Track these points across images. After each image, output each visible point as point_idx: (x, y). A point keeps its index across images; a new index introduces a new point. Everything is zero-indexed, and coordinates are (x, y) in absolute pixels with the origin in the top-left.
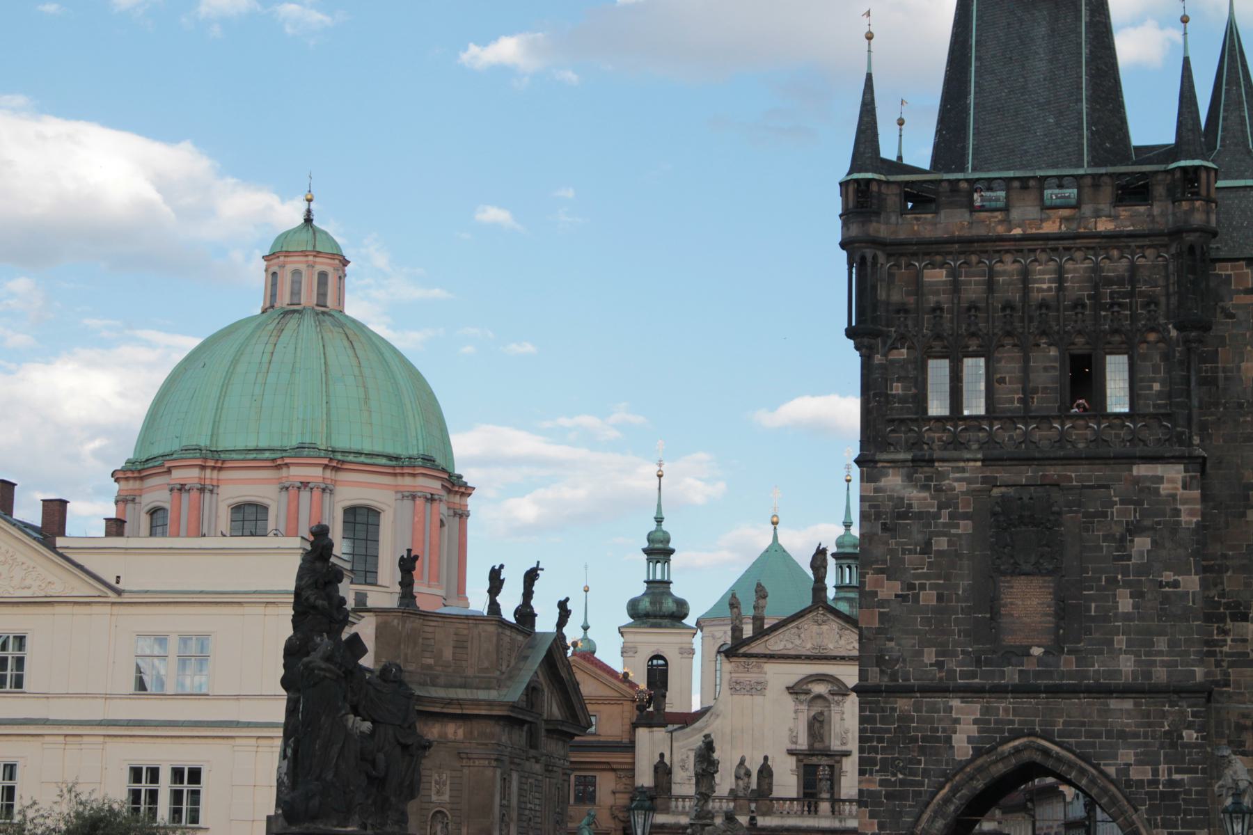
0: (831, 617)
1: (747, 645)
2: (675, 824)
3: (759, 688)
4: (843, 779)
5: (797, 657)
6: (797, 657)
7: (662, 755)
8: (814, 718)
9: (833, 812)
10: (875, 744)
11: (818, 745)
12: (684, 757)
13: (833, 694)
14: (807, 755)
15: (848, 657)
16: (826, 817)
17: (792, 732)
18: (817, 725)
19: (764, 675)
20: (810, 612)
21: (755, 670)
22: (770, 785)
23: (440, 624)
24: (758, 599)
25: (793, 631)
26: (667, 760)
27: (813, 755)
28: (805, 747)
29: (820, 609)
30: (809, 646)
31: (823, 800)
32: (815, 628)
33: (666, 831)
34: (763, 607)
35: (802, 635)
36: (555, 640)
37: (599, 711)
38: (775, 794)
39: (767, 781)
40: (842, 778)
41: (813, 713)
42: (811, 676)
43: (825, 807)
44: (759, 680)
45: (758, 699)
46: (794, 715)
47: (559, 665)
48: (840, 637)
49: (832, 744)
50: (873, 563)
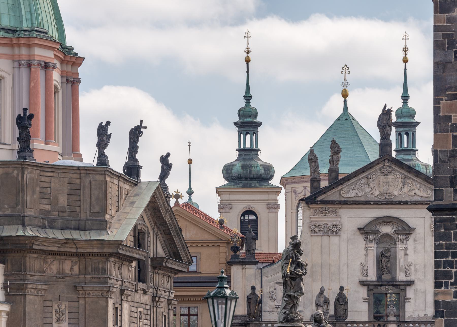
0: (396, 168)
1: (324, 193)
3: (335, 229)
4: (407, 305)
5: (367, 203)
6: (367, 203)
7: (253, 288)
8: (382, 254)
10: (450, 258)
11: (385, 277)
12: (272, 289)
13: (397, 233)
14: (376, 285)
15: (410, 202)
17: (364, 267)
18: (385, 260)
19: (339, 219)
20: (378, 164)
22: (346, 310)
23: (56, 174)
25: (363, 181)
26: (258, 292)
27: (381, 285)
29: (386, 161)
30: (377, 193)
31: (390, 322)
32: (382, 178)
34: (338, 161)
35: (371, 184)
36: (158, 188)
38: (349, 319)
41: (381, 250)
42: (378, 218)
45: (335, 240)
46: (365, 252)
47: (163, 211)
49: (398, 276)
50: (447, 90)
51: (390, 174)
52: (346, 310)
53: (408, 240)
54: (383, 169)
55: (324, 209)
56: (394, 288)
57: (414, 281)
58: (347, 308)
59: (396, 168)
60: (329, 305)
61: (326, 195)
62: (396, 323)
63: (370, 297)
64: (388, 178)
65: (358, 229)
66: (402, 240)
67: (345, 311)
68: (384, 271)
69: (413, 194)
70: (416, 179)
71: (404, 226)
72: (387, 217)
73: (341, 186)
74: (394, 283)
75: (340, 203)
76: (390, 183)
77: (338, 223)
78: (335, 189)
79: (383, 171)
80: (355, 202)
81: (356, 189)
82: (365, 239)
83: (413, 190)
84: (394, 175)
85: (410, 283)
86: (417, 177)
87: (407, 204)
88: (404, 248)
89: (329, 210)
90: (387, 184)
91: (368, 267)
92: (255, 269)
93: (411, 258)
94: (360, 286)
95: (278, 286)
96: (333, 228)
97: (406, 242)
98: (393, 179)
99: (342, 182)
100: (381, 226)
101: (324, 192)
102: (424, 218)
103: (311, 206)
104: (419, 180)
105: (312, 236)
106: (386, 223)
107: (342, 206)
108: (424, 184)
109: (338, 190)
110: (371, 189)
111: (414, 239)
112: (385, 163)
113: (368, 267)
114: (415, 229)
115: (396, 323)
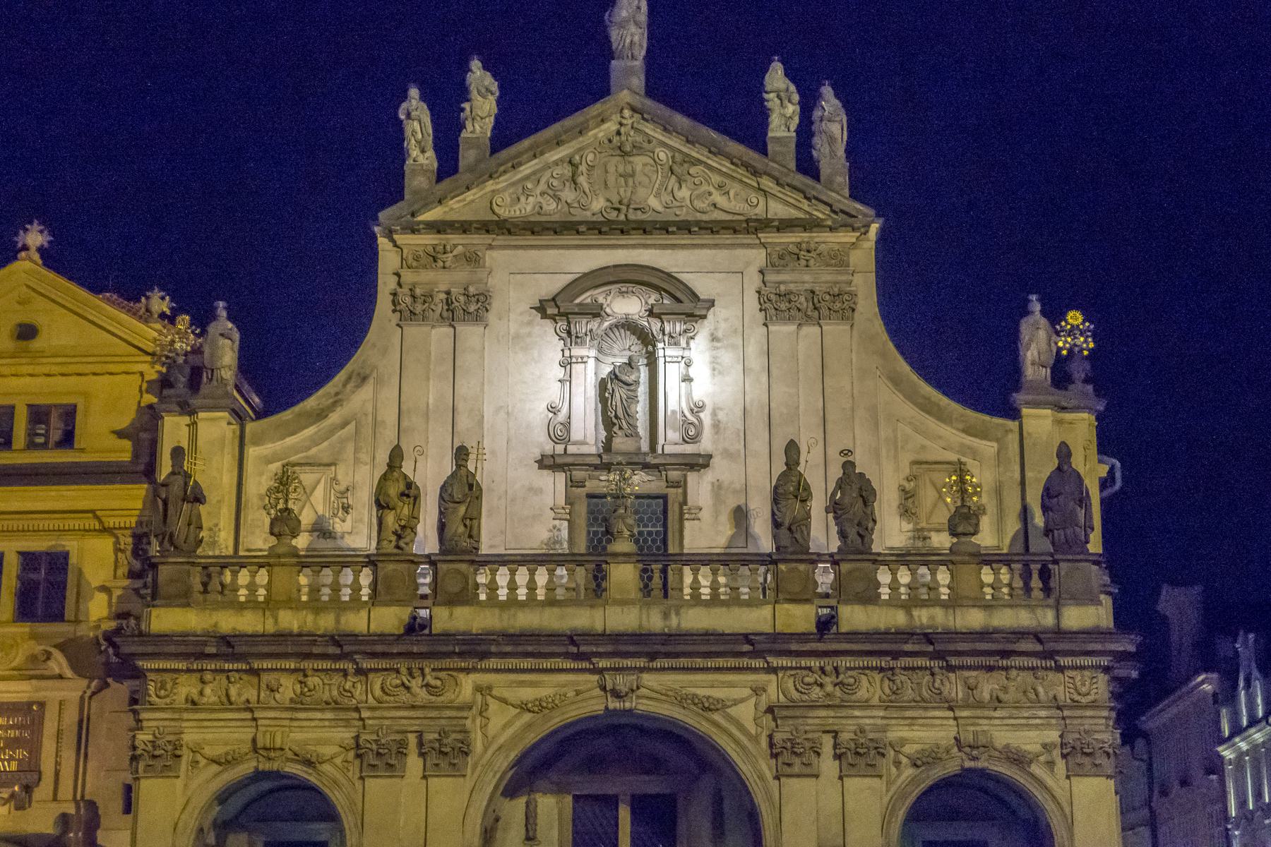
0: (658, 134)
2: (207, 634)
7: (177, 453)
8: (614, 376)
9: (646, 590)
13: (658, 316)
16: (624, 603)
18: (621, 392)
25: (557, 171)
27: (607, 467)
28: (585, 450)
30: (598, 204)
32: (615, 164)
33: (172, 649)
35: (582, 180)
37: (86, 395)
39: (462, 509)
40: (687, 524)
43: (623, 575)
44: (472, 290)
46: (560, 373)
52: (471, 519)
53: (692, 338)
56: (650, 478)
57: (710, 456)
58: (475, 514)
61: (447, 209)
63: (577, 507)
64: (629, 162)
68: (620, 428)
70: (714, 164)
72: (626, 265)
75: (485, 227)
81: (538, 192)
85: (699, 463)
89: (455, 253)
92: (224, 424)
97: (688, 343)
98: (645, 165)
104: (724, 166)
107: (494, 240)
108: (739, 176)
110: (584, 192)
111: (712, 334)
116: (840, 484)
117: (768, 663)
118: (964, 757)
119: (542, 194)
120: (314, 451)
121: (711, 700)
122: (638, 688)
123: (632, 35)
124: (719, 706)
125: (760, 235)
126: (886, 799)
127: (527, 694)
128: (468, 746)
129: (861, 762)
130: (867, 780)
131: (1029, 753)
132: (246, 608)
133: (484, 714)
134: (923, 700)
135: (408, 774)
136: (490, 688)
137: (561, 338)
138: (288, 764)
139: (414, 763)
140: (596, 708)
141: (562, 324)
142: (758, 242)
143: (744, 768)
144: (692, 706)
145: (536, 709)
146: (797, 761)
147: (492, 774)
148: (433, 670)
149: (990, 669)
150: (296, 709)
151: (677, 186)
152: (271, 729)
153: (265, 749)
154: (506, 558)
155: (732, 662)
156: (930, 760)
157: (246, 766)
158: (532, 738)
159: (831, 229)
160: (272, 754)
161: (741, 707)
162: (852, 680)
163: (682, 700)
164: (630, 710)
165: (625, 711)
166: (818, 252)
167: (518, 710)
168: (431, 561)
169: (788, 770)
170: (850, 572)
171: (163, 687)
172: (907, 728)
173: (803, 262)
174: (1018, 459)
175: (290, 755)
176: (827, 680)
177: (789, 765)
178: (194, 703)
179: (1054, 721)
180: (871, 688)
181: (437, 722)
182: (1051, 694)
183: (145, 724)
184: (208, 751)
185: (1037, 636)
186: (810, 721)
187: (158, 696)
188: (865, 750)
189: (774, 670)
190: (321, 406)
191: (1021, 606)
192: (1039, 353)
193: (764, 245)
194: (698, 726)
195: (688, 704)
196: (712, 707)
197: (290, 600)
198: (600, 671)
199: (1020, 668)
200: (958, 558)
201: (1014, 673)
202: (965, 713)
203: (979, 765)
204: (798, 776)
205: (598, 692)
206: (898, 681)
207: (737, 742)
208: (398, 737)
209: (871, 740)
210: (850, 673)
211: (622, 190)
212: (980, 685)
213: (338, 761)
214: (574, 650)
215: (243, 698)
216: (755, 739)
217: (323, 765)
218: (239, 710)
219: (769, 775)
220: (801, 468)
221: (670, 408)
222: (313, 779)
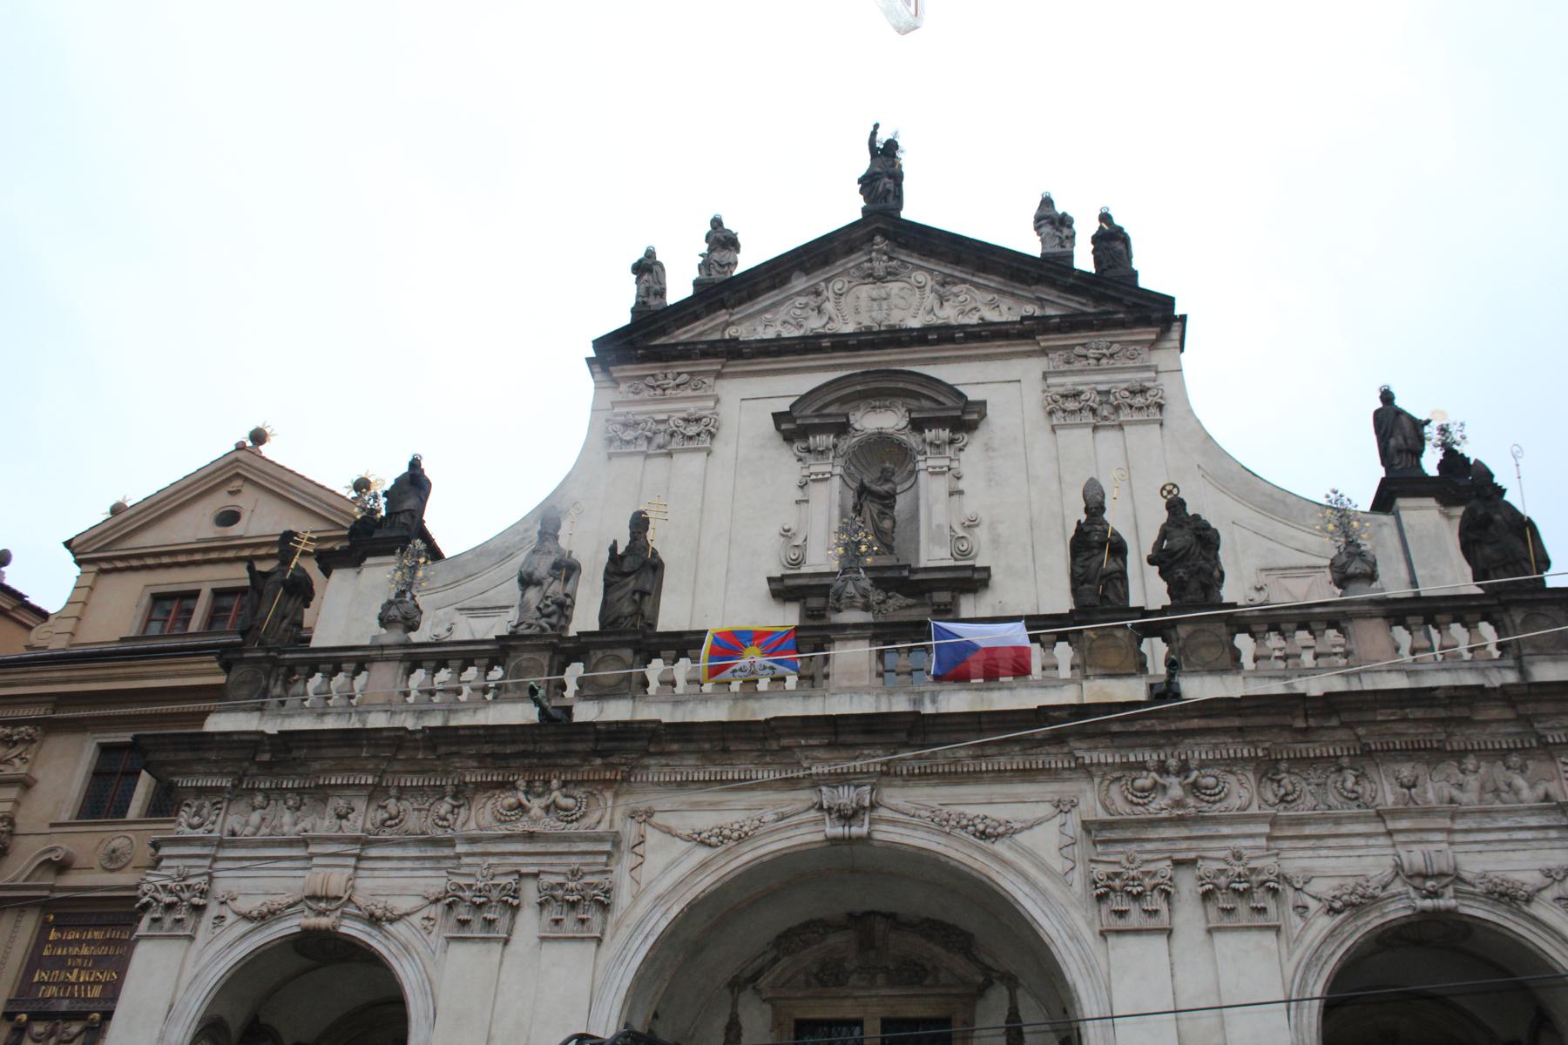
3: (692, 430)
8: (863, 492)
13: (917, 425)
15: (962, 327)
16: (854, 691)
18: (871, 508)
19: (711, 404)
20: (850, 250)
21: (689, 393)
24: (711, 250)
25: (803, 300)
29: (878, 239)
30: (849, 328)
32: (866, 291)
35: (829, 307)
39: (632, 583)
43: (853, 656)
45: (689, 464)
46: (799, 495)
48: (942, 300)
51: (893, 278)
52: (644, 594)
53: (961, 450)
54: (869, 264)
55: (660, 376)
56: (910, 601)
57: (987, 569)
59: (913, 261)
60: (571, 581)
62: (869, 633)
65: (774, 415)
66: (938, 442)
67: (637, 597)
69: (973, 319)
70: (981, 281)
71: (941, 399)
73: (724, 311)
74: (906, 573)
76: (895, 300)
77: (704, 413)
78: (702, 321)
79: (869, 269)
80: (766, 344)
81: (778, 323)
82: (802, 455)
83: (974, 312)
84: (908, 280)
85: (973, 581)
86: (984, 272)
87: (952, 340)
88: (946, 469)
90: (884, 304)
91: (806, 540)
93: (971, 505)
94: (772, 602)
95: (464, 617)
96: (685, 429)
98: (903, 289)
99: (726, 294)
100: (858, 414)
101: (660, 324)
102: (1018, 384)
103: (619, 371)
105: (610, 457)
106: (877, 403)
107: (723, 367)
108: (1010, 290)
109: (714, 329)
111: (986, 444)
112: (873, 245)
113: (806, 540)
114: (984, 403)
115: (869, 633)
116: (1164, 534)
117: (1078, 758)
118: (1413, 894)
119: (784, 322)
120: (492, 592)
121: (988, 821)
122: (873, 806)
123: (885, 184)
124: (1001, 830)
125: (1038, 338)
126: (1289, 968)
127: (705, 821)
128: (607, 892)
129: (1243, 908)
130: (1254, 936)
131: (1523, 884)
132: (329, 714)
133: (636, 849)
134: (1330, 808)
135: (515, 938)
136: (650, 813)
137: (800, 460)
138: (346, 922)
139: (529, 923)
140: (809, 838)
141: (799, 445)
142: (1036, 348)
143: (1049, 925)
144: (958, 831)
145: (714, 840)
146: (1134, 909)
147: (641, 938)
148: (565, 784)
149: (1435, 755)
150: (365, 842)
151: (936, 304)
152: (329, 870)
153: (314, 897)
154: (686, 638)
155: (1018, 762)
156: (1354, 899)
157: (288, 924)
158: (706, 882)
159: (1122, 325)
160: (323, 905)
161: (1036, 829)
162: (1211, 781)
163: (942, 824)
164: (860, 839)
165: (849, 840)
166: (1111, 351)
167: (690, 844)
168: (582, 648)
169: (1120, 924)
170: (1189, 637)
171: (197, 814)
172: (1310, 853)
173: (1092, 362)
174: (1401, 556)
175: (351, 909)
176: (1173, 781)
177: (1121, 914)
178: (233, 834)
179: (1553, 834)
180: (1241, 791)
181: (565, 860)
182: (1540, 790)
183: (164, 863)
184: (244, 905)
185: (1504, 694)
186: (1149, 846)
187: (192, 827)
188: (1245, 885)
189: (1086, 770)
190: (506, 544)
191: (1461, 669)
192: (1405, 440)
193: (1044, 352)
194: (969, 861)
195: (954, 827)
196: (988, 830)
197: (390, 702)
198: (815, 783)
199: (1485, 754)
200: (1355, 608)
201: (1470, 763)
202: (1404, 824)
203: (1441, 903)
204: (1137, 932)
205: (813, 814)
206: (1285, 782)
207: (1033, 885)
208: (503, 881)
209: (1253, 870)
210: (1209, 771)
211: (874, 314)
212: (1420, 782)
213: (416, 919)
214: (775, 746)
215: (299, 827)
216: (1063, 878)
217: (395, 924)
218: (290, 843)
219: (1089, 937)
220: (1106, 516)
221: (935, 522)
222: (375, 941)
